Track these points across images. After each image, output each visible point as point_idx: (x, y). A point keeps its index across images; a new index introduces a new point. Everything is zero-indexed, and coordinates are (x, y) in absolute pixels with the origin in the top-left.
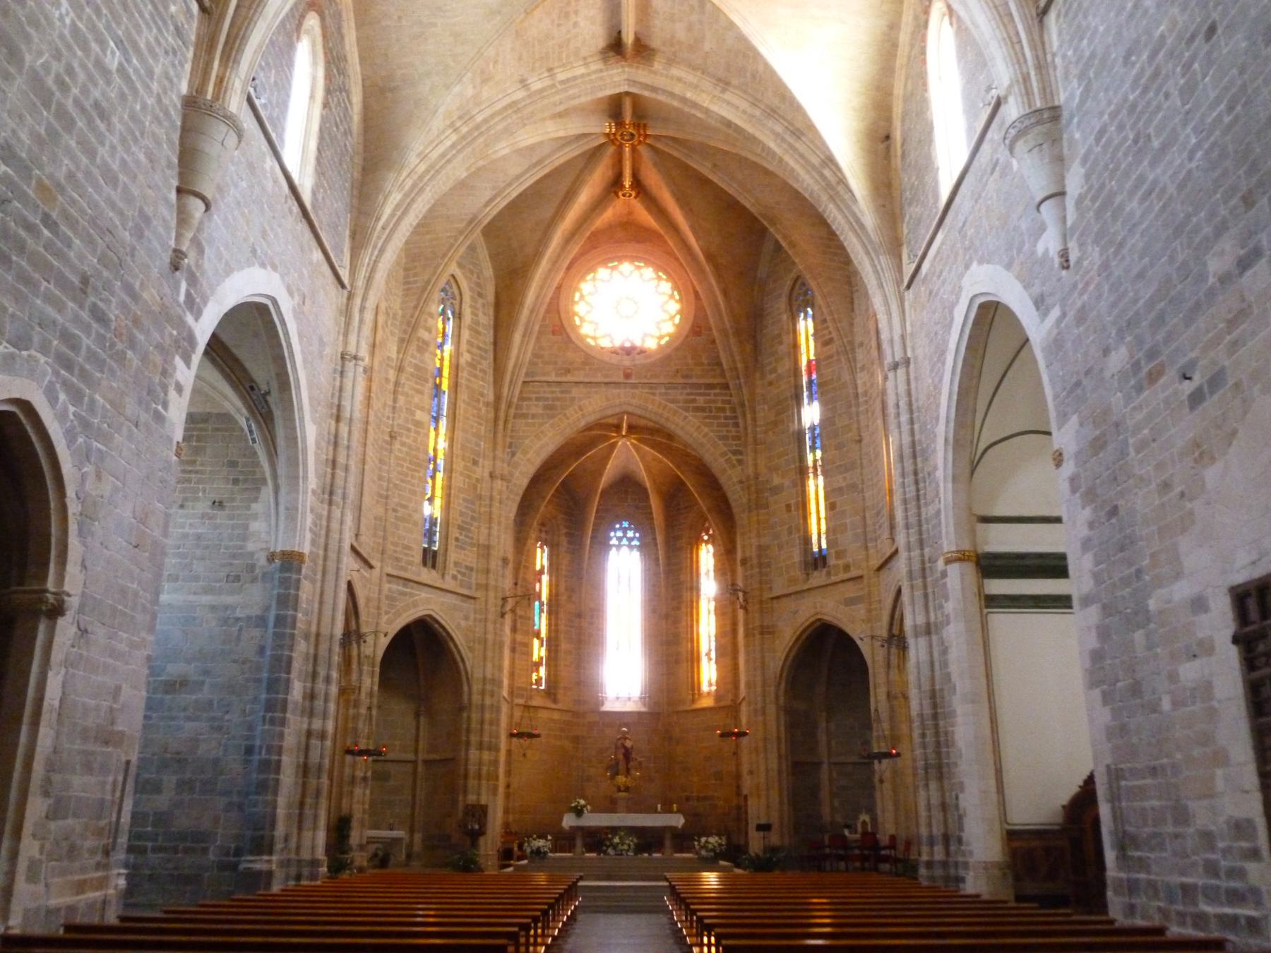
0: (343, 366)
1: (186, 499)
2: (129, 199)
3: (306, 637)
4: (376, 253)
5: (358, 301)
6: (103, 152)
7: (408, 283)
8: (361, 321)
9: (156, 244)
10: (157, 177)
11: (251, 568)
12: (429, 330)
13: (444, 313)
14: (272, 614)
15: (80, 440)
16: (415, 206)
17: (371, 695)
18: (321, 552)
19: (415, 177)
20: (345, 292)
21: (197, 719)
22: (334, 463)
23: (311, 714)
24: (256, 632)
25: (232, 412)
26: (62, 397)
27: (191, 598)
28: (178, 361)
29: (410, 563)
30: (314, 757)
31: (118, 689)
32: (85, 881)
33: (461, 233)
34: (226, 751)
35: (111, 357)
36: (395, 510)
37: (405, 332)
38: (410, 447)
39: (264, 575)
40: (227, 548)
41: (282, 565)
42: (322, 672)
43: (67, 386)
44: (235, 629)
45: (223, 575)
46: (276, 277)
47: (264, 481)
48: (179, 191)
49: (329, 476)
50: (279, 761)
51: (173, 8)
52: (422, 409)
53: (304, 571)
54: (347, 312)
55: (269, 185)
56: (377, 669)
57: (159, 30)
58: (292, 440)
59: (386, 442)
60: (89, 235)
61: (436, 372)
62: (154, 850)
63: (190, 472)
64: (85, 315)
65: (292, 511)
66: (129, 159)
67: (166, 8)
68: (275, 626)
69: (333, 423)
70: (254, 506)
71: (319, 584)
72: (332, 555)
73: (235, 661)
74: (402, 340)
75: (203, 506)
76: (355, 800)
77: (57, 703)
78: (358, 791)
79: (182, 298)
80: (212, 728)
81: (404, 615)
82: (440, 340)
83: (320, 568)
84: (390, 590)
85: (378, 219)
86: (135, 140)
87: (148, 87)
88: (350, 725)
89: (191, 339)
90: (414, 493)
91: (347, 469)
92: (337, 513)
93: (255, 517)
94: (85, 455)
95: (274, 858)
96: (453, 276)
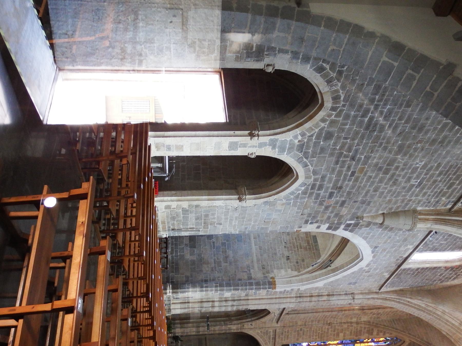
0: (349, 294)
1: (288, 248)
2: (372, 197)
3: (247, 295)
4: (397, 300)
5: (376, 296)
6: (383, 185)
7: (394, 321)
8: (369, 299)
9: (362, 209)
10: (384, 206)
11: (268, 272)
12: (378, 334)
13: (387, 340)
14: (254, 281)
15: (292, 197)
16: (422, 313)
17: (230, 329)
18: (278, 296)
19: (434, 311)
20: (378, 291)
21: (215, 263)
22: (312, 296)
23: (220, 301)
24: (246, 277)
25: (322, 257)
26: (303, 188)
27: (255, 255)
28: (327, 225)
29: (282, 340)
30: (205, 305)
31: (221, 224)
32: (165, 224)
33: (422, 339)
34: (206, 273)
35: (320, 201)
36: (301, 329)
37: (373, 323)
38: (327, 333)
39: (266, 277)
40: (273, 263)
41: (270, 282)
42: (235, 303)
43: (307, 189)
44: (246, 270)
45: (264, 263)
46: (371, 258)
47: (300, 272)
48: (383, 214)
49: (306, 295)
50: (203, 291)
51: (444, 199)
52: (344, 336)
53: (270, 290)
54: (370, 292)
55: (402, 249)
56: (239, 331)
57: (433, 196)
58: (316, 277)
59: (327, 322)
60: (355, 186)
61: (361, 340)
62: (172, 256)
63: (297, 247)
64: (330, 190)
65: (290, 282)
66: (385, 194)
67: (443, 196)
68: (249, 283)
69: (326, 294)
70: (290, 270)
71: (266, 297)
72: (277, 301)
73: (235, 271)
74: (369, 322)
75: (286, 254)
76: (191, 329)
77: (215, 205)
78: (194, 329)
79: (348, 222)
80: (212, 268)
81: (261, 340)
82: (375, 340)
83: (272, 297)
84: (270, 332)
85: (411, 298)
86: (392, 195)
87: (411, 195)
88: (218, 323)
89: (336, 229)
90: (310, 337)
91: (310, 301)
92: (293, 300)
93: (286, 271)
94: (287, 198)
95: (171, 294)
96: (404, 342)
